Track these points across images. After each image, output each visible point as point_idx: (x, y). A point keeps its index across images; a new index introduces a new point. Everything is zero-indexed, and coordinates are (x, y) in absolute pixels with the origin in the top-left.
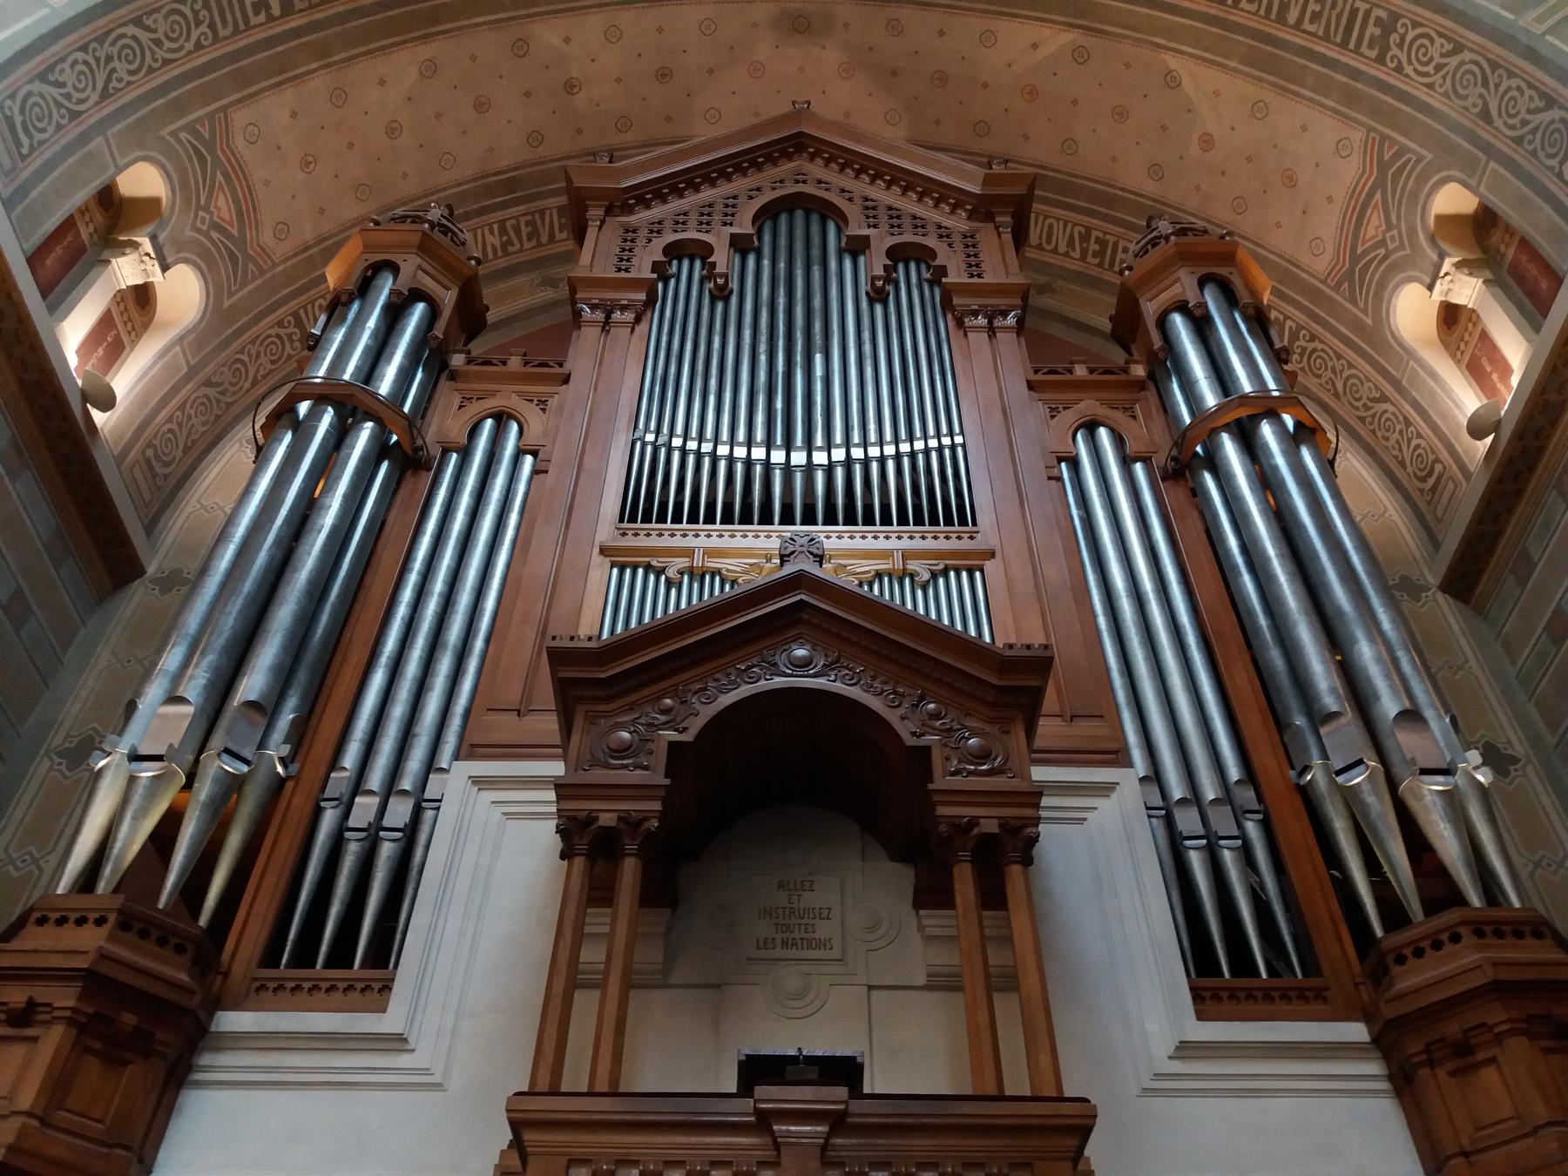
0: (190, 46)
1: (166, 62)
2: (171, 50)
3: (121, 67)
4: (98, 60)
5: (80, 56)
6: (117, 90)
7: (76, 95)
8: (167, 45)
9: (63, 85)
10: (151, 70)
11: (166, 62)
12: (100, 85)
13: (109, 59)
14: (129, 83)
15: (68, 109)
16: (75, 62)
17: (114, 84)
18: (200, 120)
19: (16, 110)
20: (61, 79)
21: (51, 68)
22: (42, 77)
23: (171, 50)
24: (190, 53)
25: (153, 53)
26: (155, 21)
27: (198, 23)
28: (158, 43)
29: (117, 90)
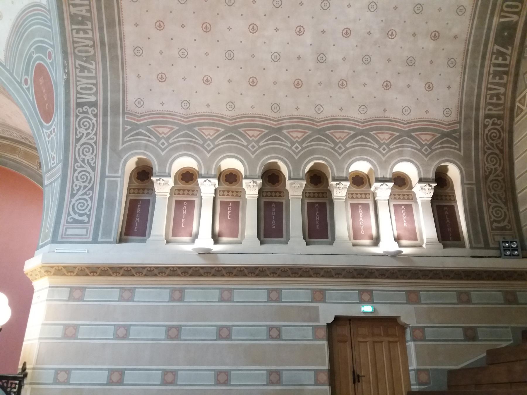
0: (94, 120)
1: (96, 134)
2: (92, 130)
3: (89, 157)
4: (82, 166)
5: (76, 174)
6: (95, 163)
7: (86, 184)
8: (90, 131)
9: (80, 187)
10: (95, 143)
11: (96, 134)
12: (89, 170)
13: (83, 161)
14: (95, 156)
15: (89, 190)
16: (77, 177)
17: (92, 162)
18: (124, 128)
19: (73, 215)
20: (78, 187)
21: (73, 190)
22: (73, 196)
23: (92, 130)
24: (97, 121)
25: (90, 139)
26: (80, 133)
27: (87, 113)
28: (88, 134)
29: (95, 163)
